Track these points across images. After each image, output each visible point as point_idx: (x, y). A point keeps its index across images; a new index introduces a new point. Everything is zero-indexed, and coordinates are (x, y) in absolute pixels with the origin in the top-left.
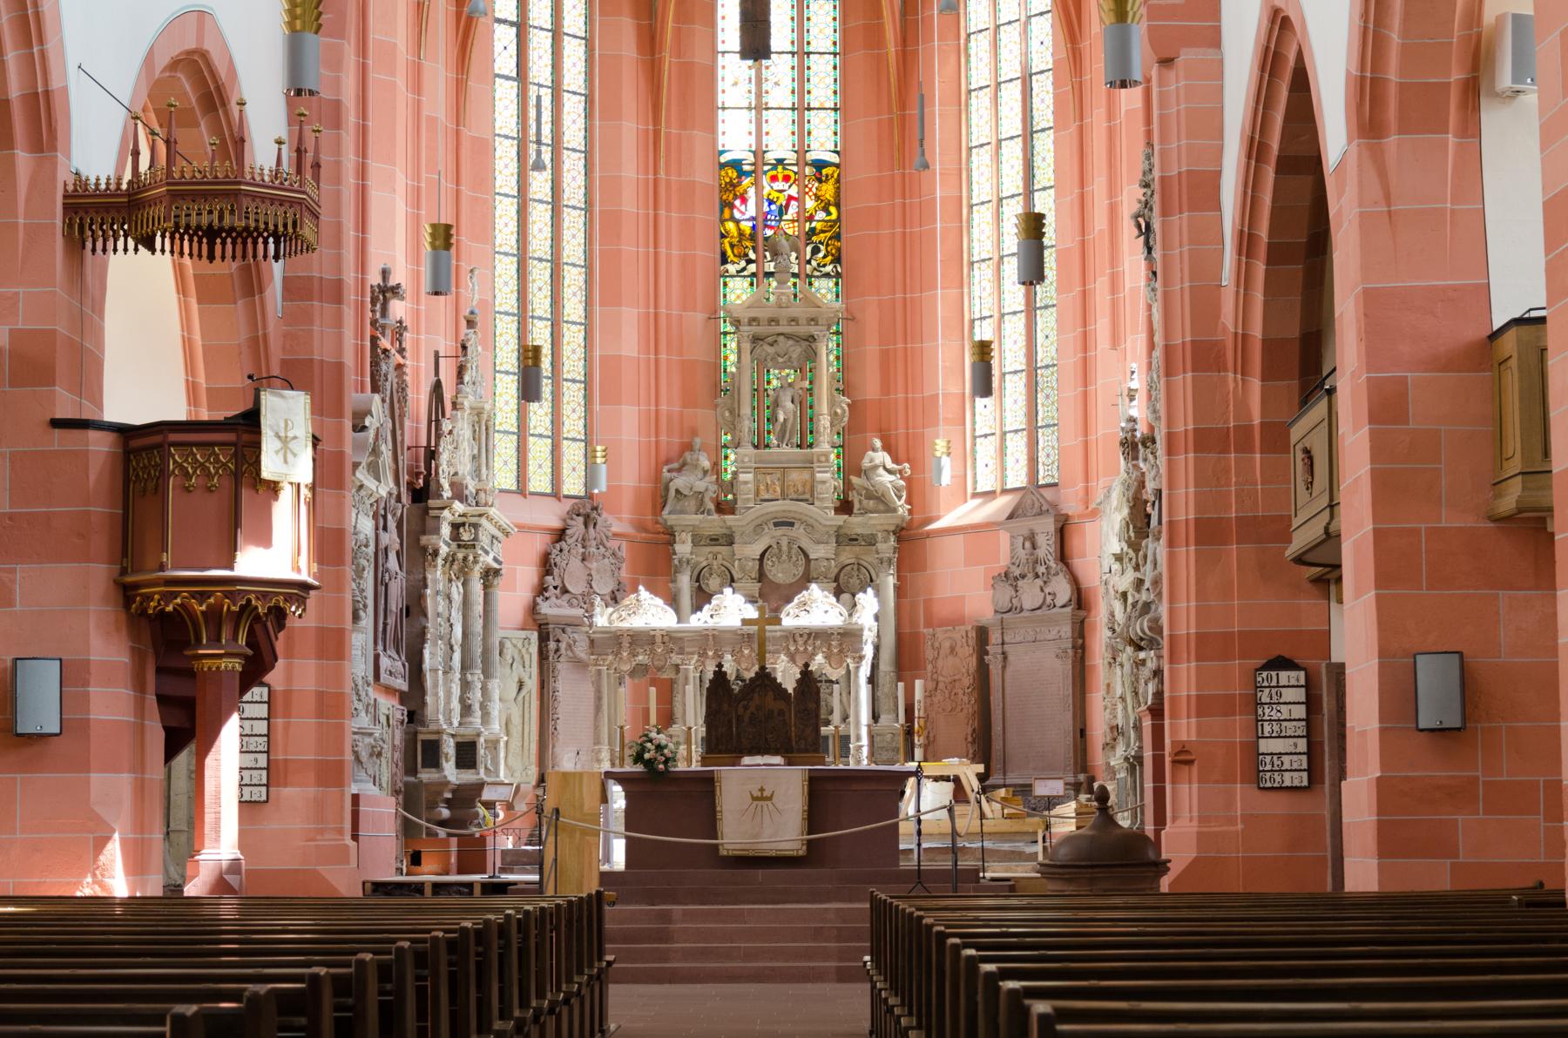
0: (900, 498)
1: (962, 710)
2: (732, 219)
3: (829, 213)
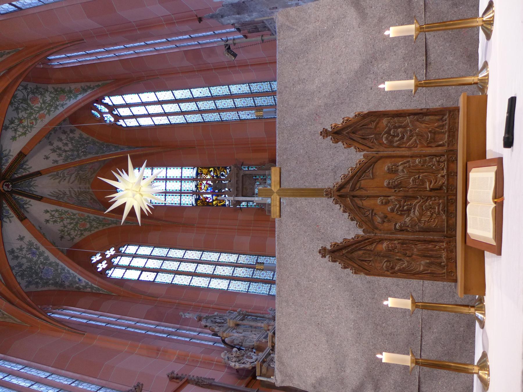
2: (212, 202)
3: (211, 171)
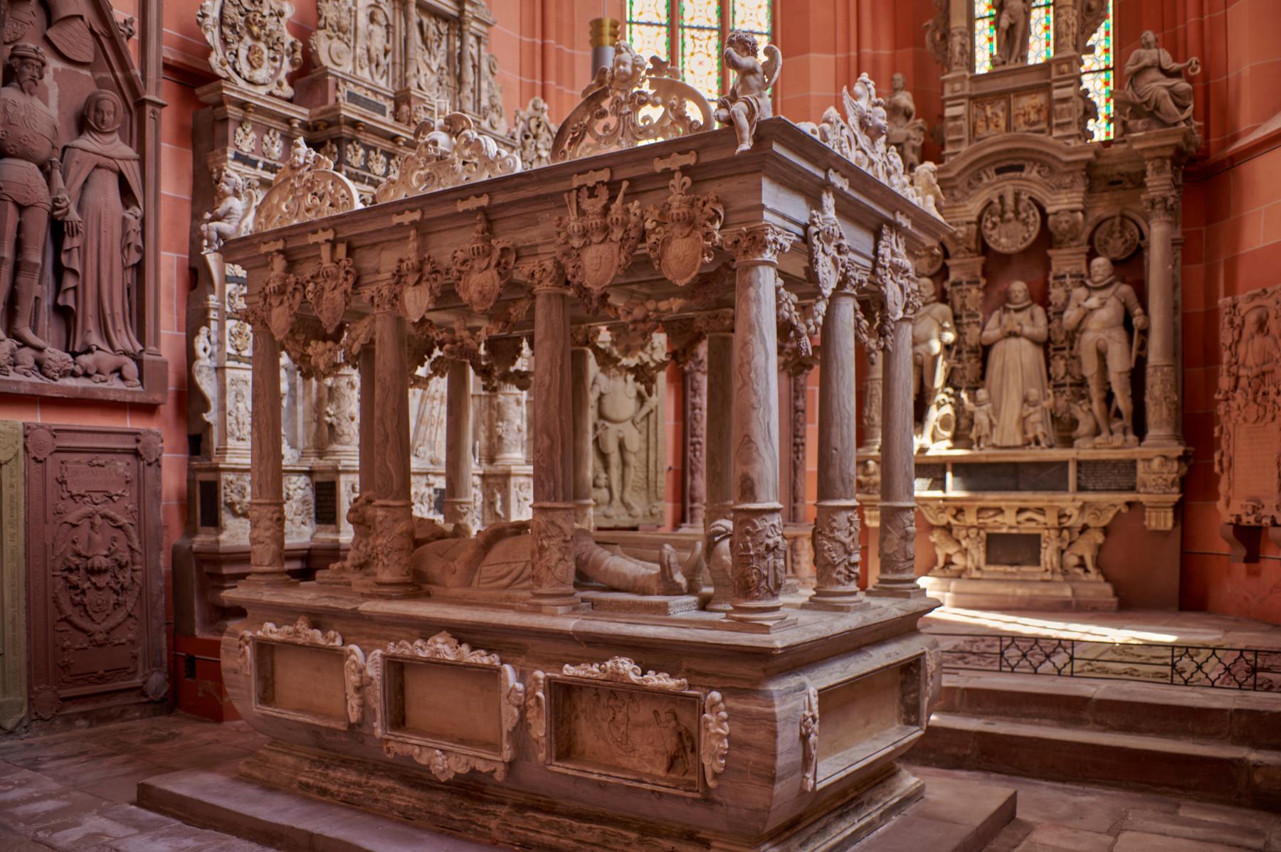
0: (1182, 108)
1: (1273, 419)
